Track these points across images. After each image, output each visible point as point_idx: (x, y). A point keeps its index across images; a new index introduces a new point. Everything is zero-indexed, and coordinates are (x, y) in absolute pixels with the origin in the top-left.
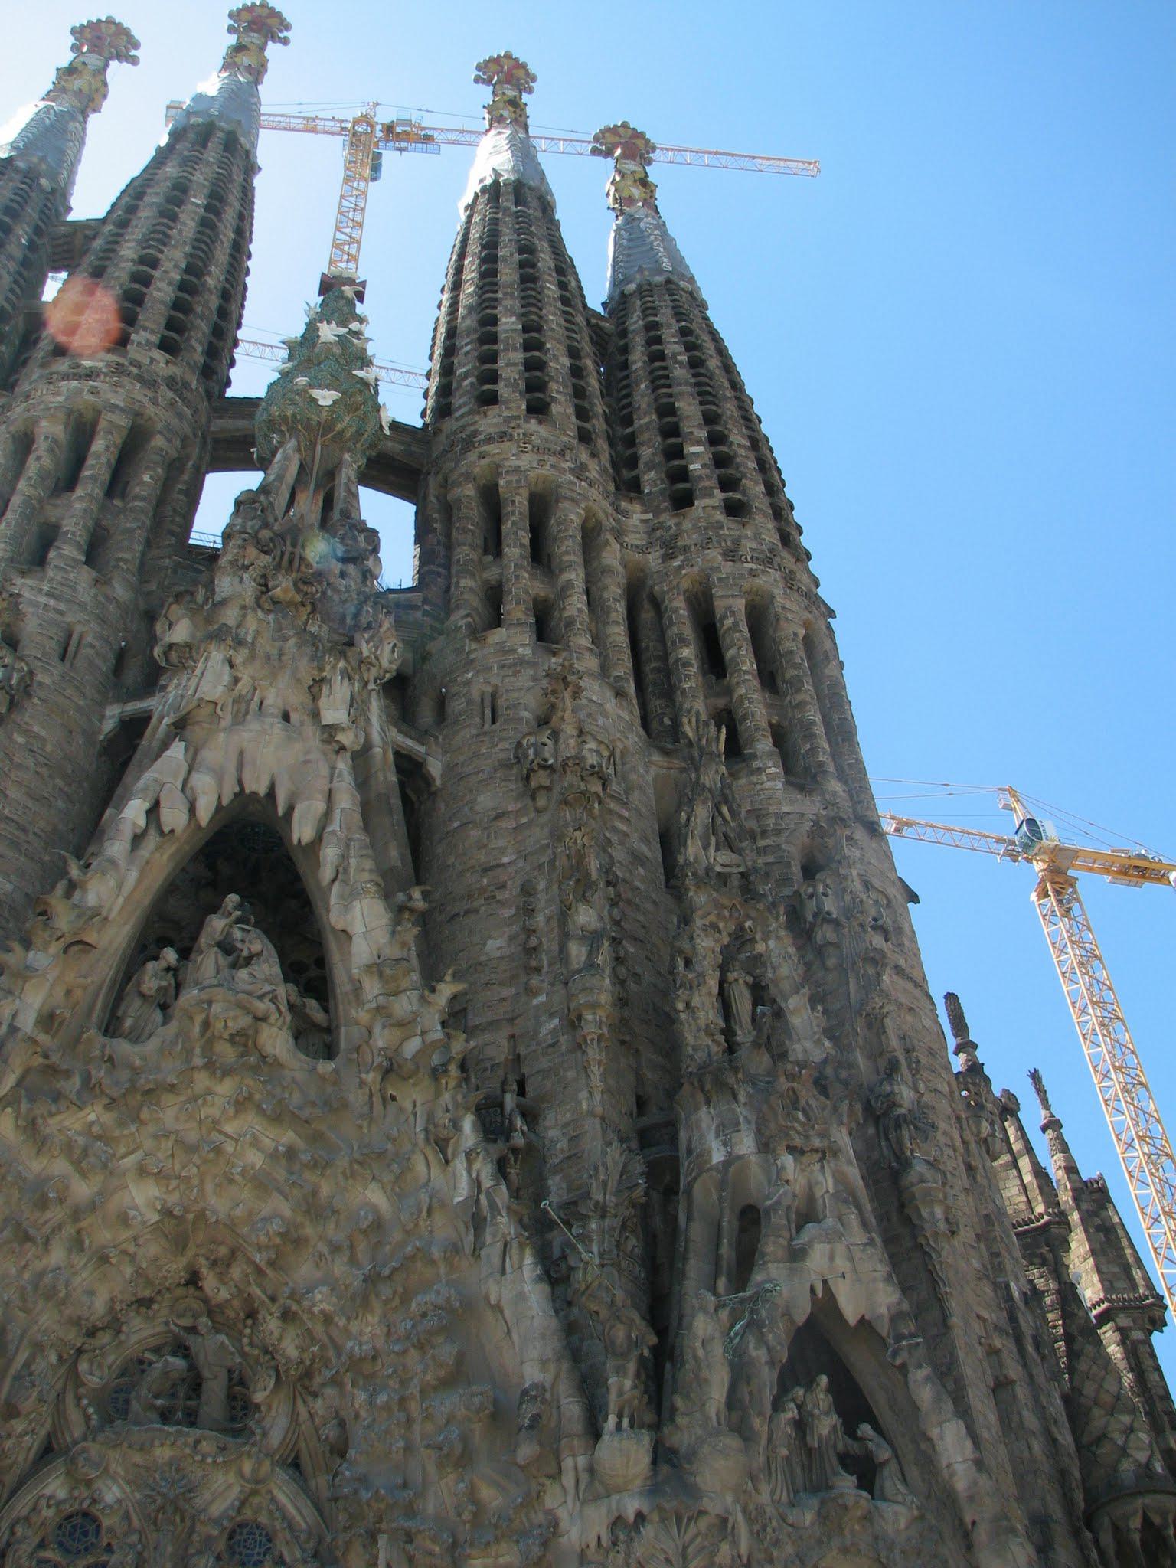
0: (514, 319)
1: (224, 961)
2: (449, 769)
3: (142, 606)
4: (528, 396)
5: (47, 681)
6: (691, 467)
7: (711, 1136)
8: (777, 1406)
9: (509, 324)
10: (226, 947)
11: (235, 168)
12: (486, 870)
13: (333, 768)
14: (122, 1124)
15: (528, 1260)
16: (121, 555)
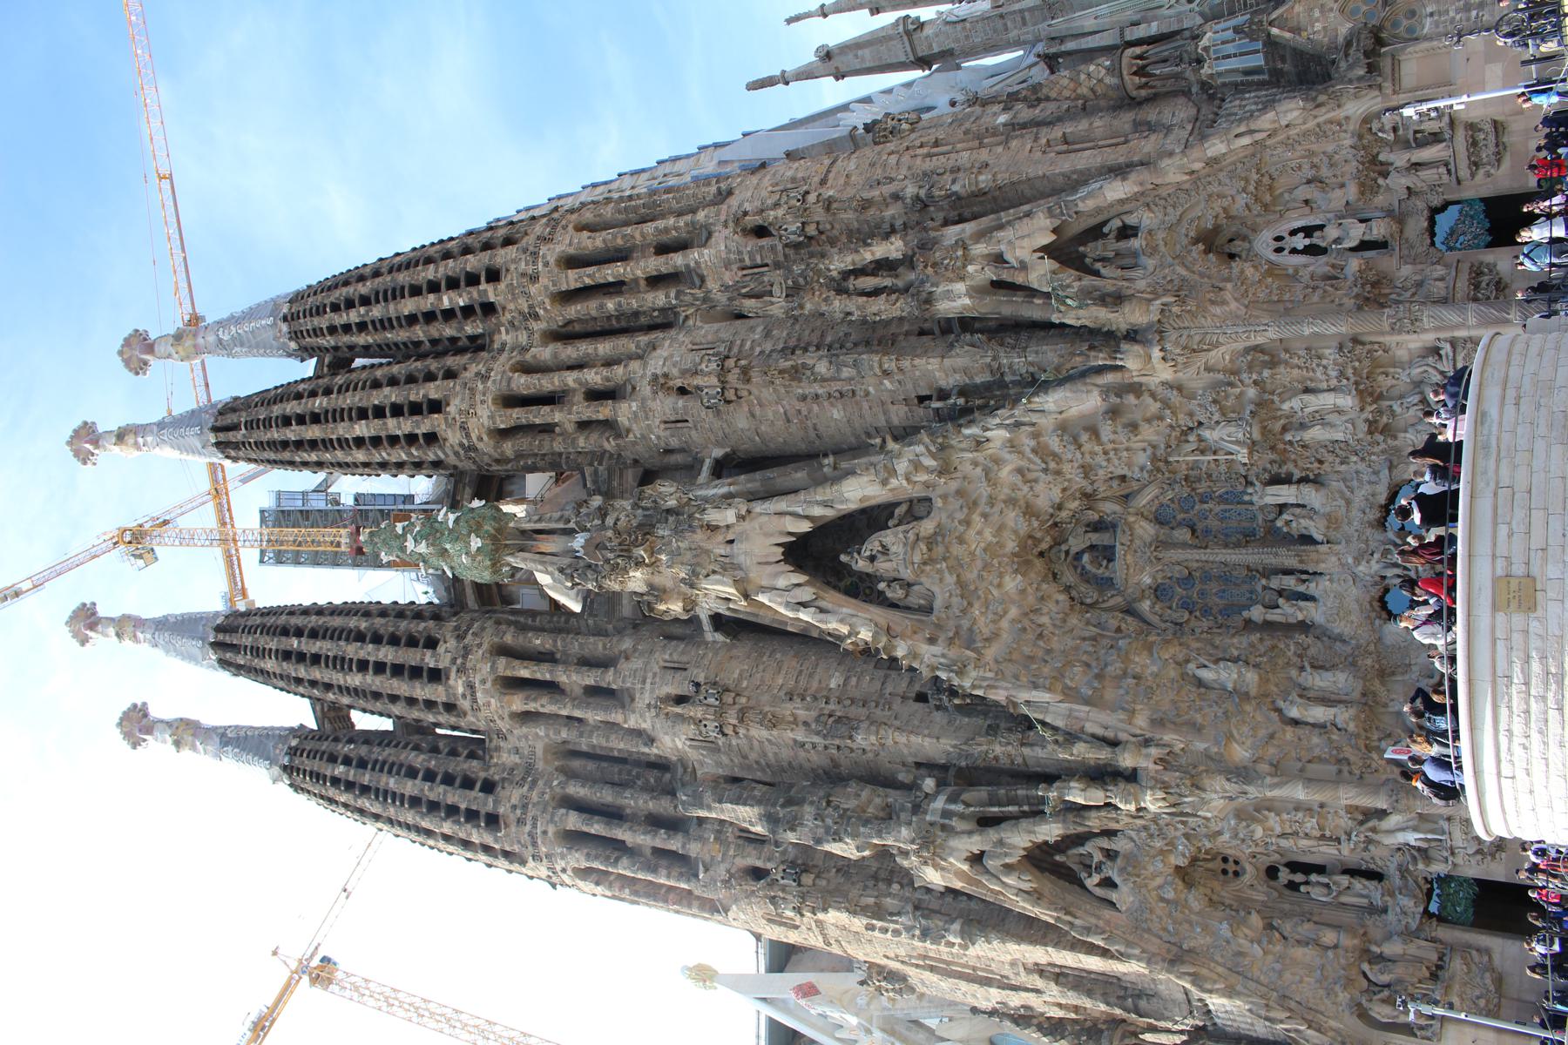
0: (356, 426)
1: (881, 558)
2: (718, 444)
3: (631, 631)
4: (425, 413)
5: (703, 675)
6: (462, 304)
7: (954, 304)
8: (1097, 274)
9: (361, 429)
10: (872, 559)
11: (249, 623)
12: (788, 421)
13: (761, 514)
14: (979, 598)
15: (1037, 399)
16: (600, 646)
